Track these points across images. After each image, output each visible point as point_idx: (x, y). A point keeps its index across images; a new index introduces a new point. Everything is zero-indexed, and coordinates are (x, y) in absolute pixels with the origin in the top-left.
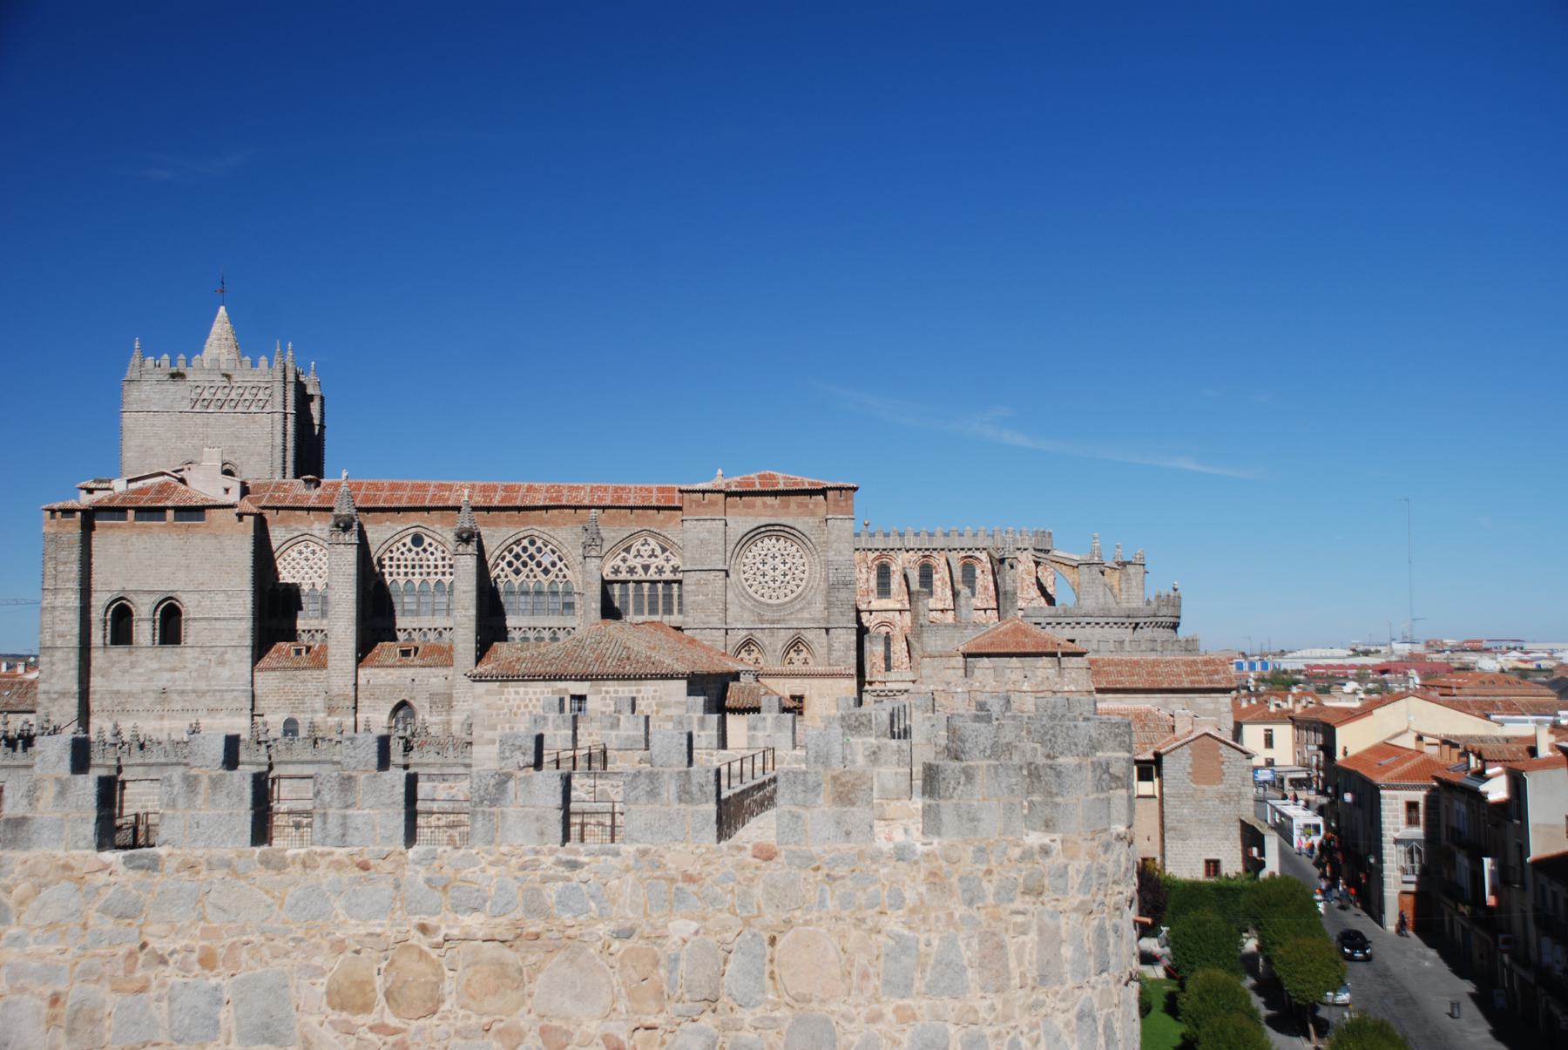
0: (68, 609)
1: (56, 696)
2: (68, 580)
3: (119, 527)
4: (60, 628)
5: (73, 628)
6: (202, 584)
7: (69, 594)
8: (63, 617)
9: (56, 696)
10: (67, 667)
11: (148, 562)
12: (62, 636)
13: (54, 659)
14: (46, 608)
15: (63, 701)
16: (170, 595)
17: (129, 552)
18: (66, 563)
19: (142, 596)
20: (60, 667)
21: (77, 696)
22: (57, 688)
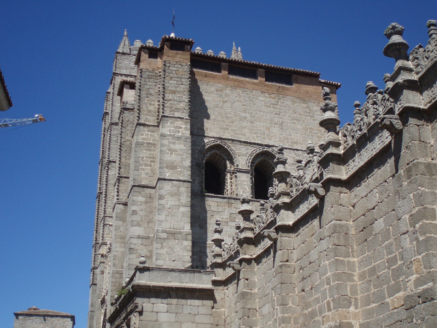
0: (179, 138)
1: (165, 235)
2: (178, 110)
3: (214, 77)
4: (168, 158)
5: (183, 160)
6: (296, 143)
7: (179, 123)
8: (172, 146)
9: (165, 235)
10: (177, 203)
11: (243, 114)
12: (172, 167)
13: (163, 192)
14: (143, 144)
15: (172, 243)
16: (266, 149)
17: (224, 102)
18: (174, 92)
19: (239, 146)
20: (169, 202)
21: (190, 237)
22: (166, 226)
